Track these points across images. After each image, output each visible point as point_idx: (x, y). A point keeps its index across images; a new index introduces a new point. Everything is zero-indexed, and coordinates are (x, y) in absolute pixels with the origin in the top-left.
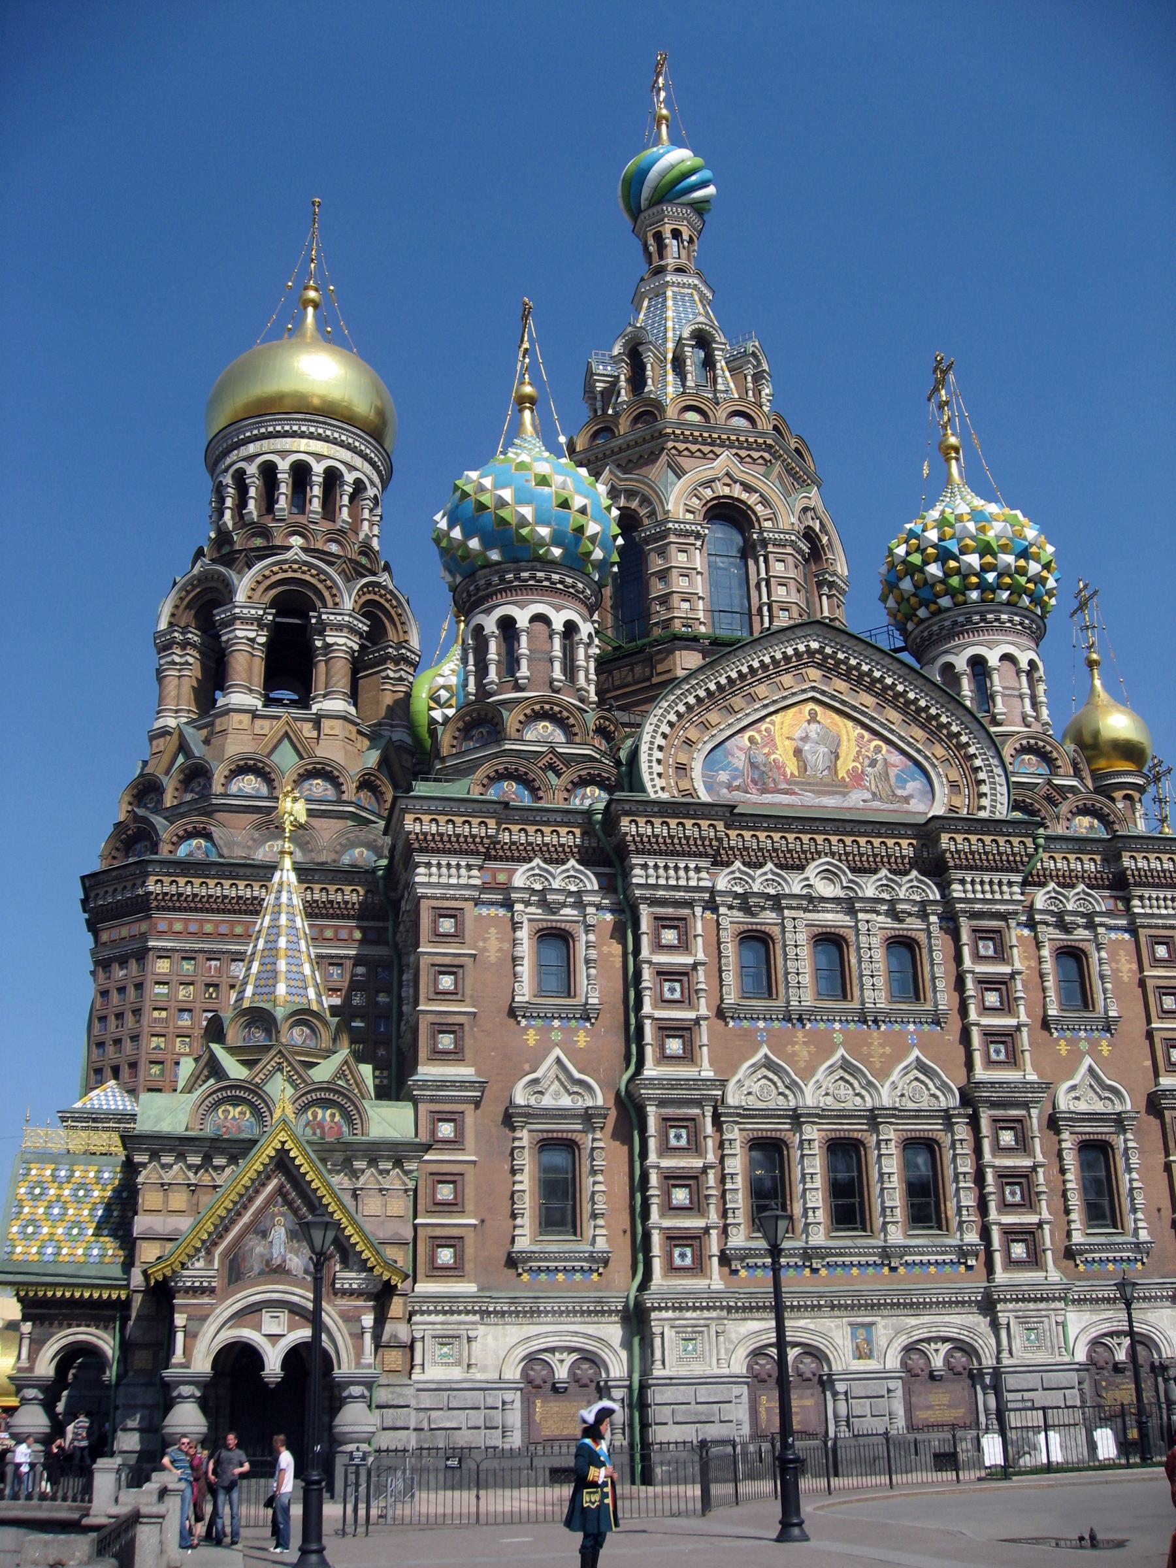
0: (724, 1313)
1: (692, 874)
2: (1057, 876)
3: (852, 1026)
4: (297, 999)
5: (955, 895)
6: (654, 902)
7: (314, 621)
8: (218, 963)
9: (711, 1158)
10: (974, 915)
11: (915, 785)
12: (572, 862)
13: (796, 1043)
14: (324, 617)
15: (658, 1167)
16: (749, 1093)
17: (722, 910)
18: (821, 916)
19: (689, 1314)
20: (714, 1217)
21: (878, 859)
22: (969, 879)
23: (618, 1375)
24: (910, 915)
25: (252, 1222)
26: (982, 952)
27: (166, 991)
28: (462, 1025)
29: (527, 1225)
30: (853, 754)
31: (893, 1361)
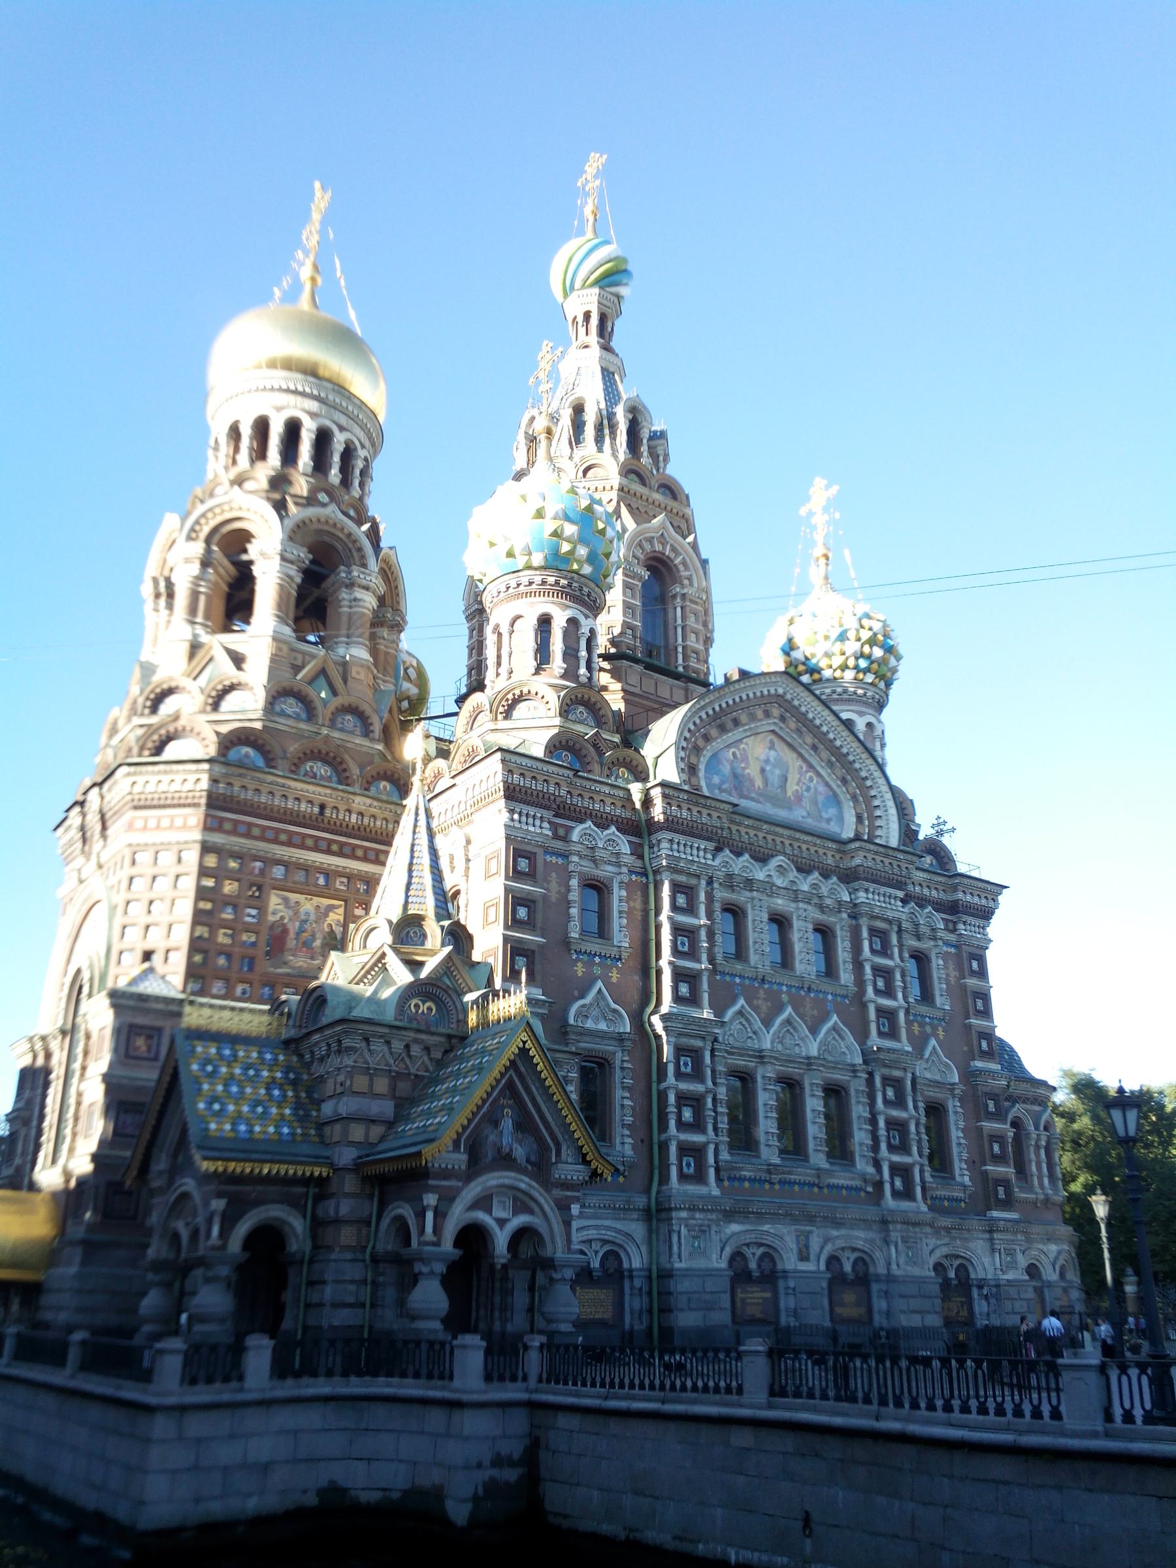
0: (721, 1216)
3: (793, 990)
7: (343, 575)
9: (710, 1083)
11: (832, 812)
12: (613, 829)
13: (758, 998)
14: (355, 574)
15: (676, 1089)
17: (716, 885)
19: (697, 1215)
23: (636, 1264)
25: (488, 1111)
28: (533, 952)
30: (796, 780)
31: (823, 1267)
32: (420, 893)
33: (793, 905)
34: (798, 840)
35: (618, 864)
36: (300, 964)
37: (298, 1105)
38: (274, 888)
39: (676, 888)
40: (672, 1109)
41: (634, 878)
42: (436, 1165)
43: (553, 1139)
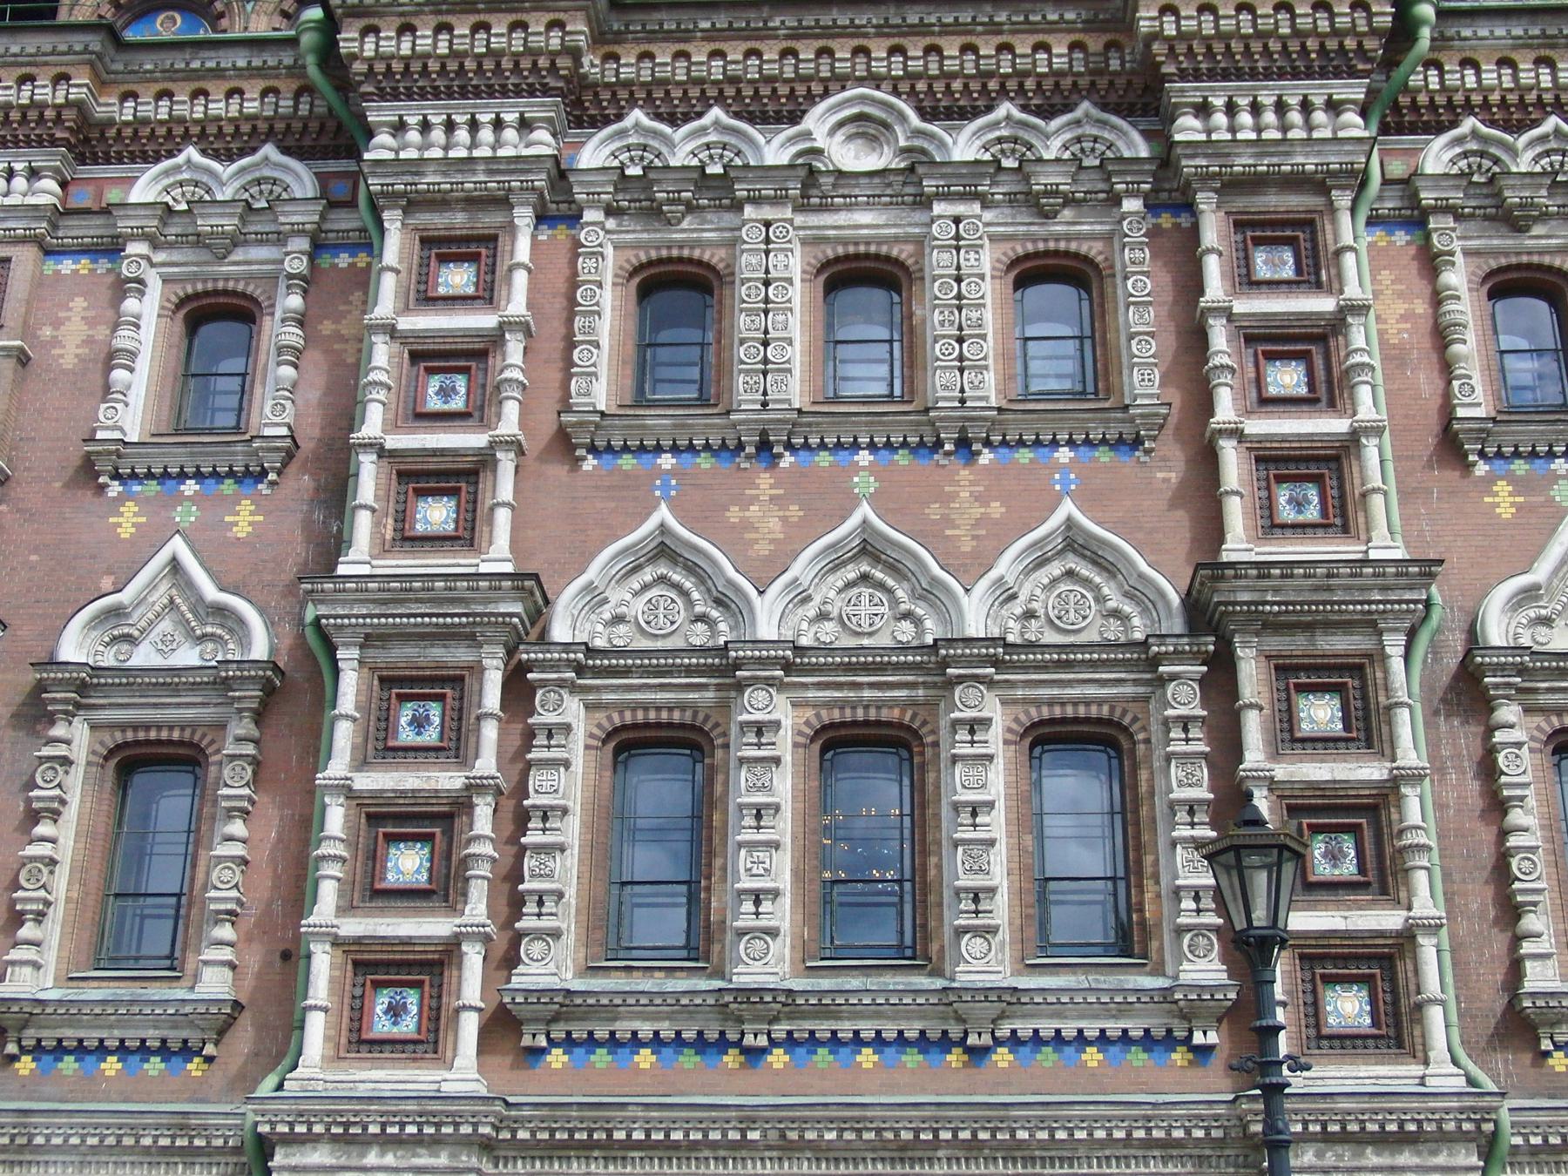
1: (510, 134)
2: (1486, 105)
3: (902, 458)
5: (1178, 137)
6: (412, 203)
9: (486, 764)
10: (1232, 186)
13: (754, 499)
16: (618, 619)
17: (590, 215)
18: (841, 218)
20: (477, 908)
21: (993, 85)
22: (1219, 102)
24: (1069, 201)
26: (1262, 271)
29: (54, 941)
33: (920, 216)
35: (280, 239)
41: (343, 260)
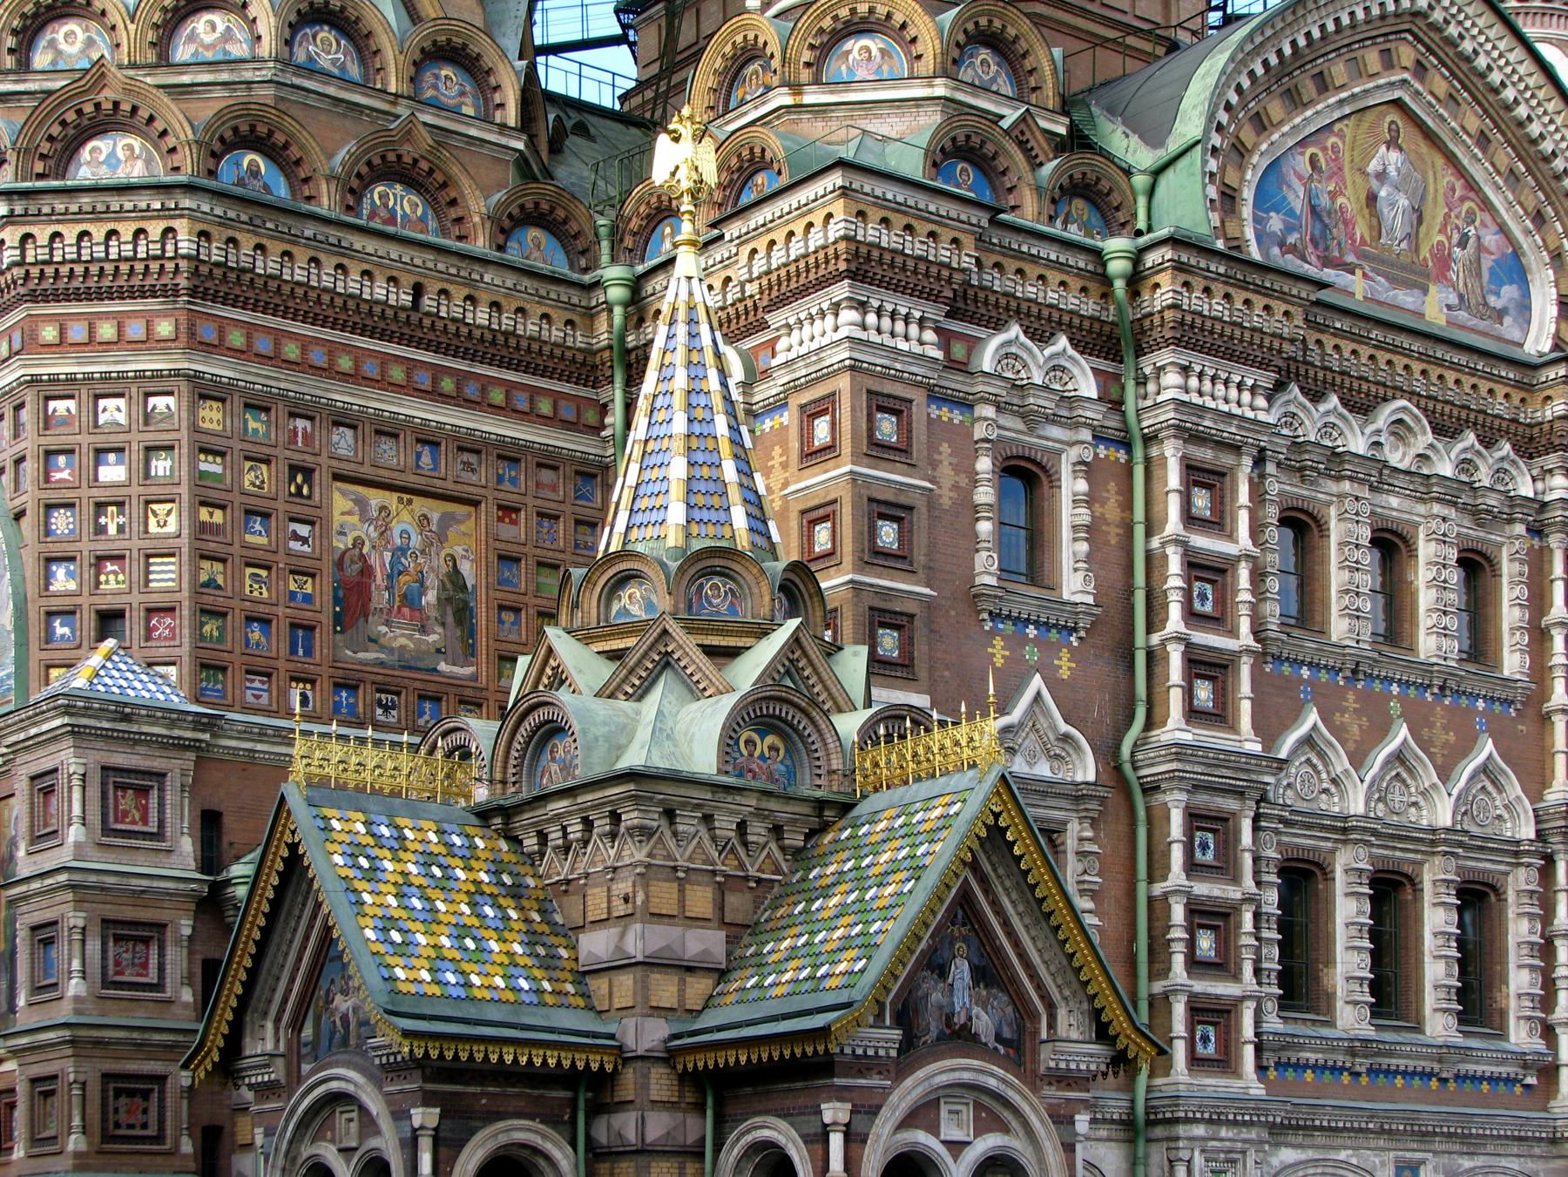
4: (760, 541)
8: (308, 424)
17: (1270, 468)
25: (929, 946)
27: (218, 469)
28: (912, 616)
32: (716, 501)
34: (1439, 362)
35: (1074, 424)
36: (403, 641)
37: (532, 938)
38: (337, 477)
39: (1195, 475)
40: (1178, 933)
41: (1102, 451)
42: (848, 1050)
43: (1042, 997)
